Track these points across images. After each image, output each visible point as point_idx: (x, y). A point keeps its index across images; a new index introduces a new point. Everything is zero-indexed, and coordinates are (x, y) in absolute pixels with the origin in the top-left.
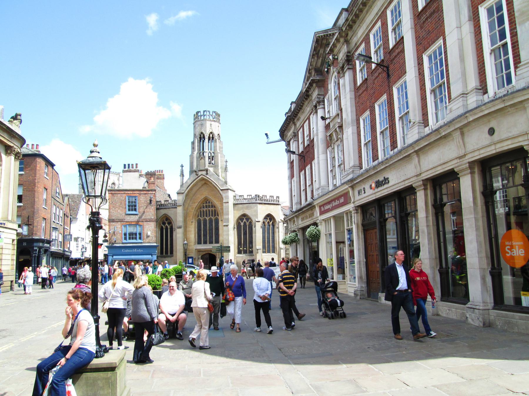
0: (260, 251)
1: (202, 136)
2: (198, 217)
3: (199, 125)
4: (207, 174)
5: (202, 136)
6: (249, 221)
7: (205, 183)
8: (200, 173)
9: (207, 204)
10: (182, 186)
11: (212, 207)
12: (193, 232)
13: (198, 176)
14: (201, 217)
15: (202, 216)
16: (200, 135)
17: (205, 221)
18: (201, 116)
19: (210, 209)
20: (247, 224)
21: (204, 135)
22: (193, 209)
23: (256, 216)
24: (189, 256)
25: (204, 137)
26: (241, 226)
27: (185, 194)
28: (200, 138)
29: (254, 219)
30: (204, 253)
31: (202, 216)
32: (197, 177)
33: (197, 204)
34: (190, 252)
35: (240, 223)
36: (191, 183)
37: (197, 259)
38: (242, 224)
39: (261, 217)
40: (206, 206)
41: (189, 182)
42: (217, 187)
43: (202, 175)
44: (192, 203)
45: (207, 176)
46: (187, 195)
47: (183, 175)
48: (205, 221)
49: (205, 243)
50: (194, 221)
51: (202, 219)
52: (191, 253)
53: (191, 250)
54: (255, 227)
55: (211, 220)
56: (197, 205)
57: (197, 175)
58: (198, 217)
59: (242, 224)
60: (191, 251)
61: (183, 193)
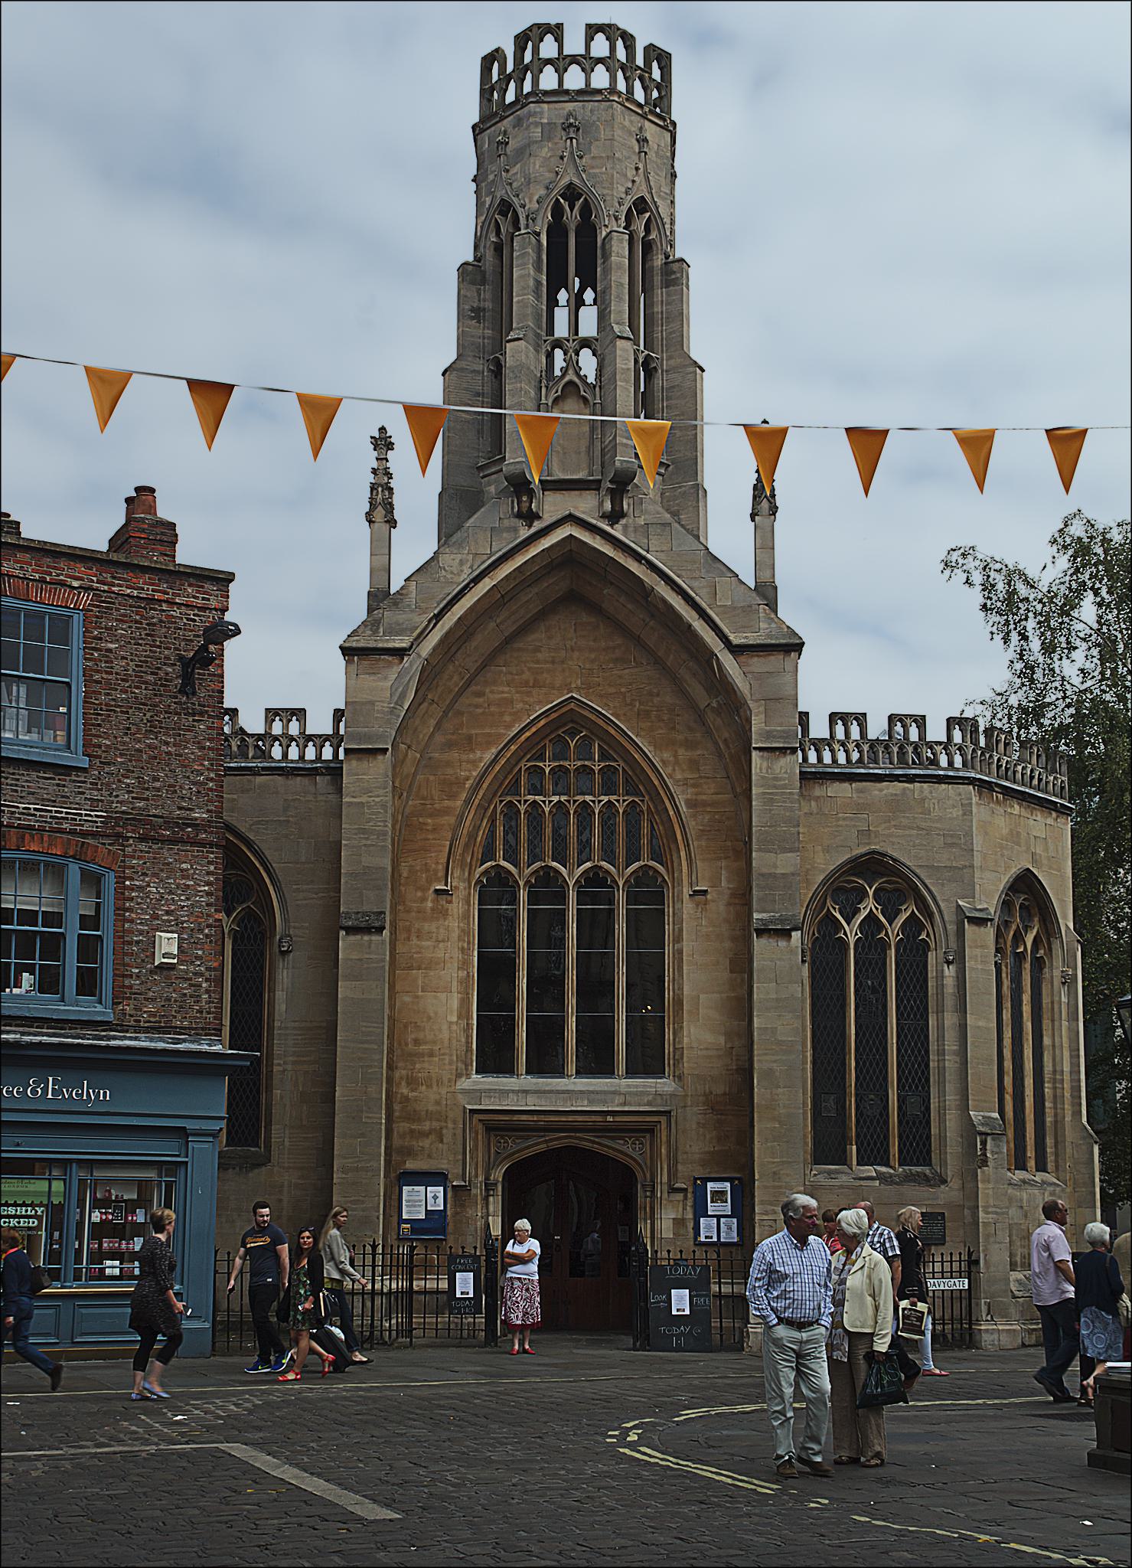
0: (998, 1151)
1: (572, 217)
2: (488, 854)
3: (548, 130)
4: (615, 516)
5: (572, 217)
6: (903, 917)
7: (573, 599)
8: (552, 506)
9: (572, 764)
10: (379, 597)
11: (609, 789)
12: (452, 974)
13: (537, 526)
14: (512, 856)
15: (524, 856)
16: (557, 211)
17: (547, 887)
18: (561, 63)
19: (597, 801)
20: (893, 932)
21: (586, 211)
22: (453, 796)
23: (963, 876)
24: (411, 1165)
25: (588, 228)
26: (844, 944)
27: (413, 665)
28: (557, 230)
29: (945, 898)
30: (536, 1145)
31: (524, 856)
32: (525, 533)
33: (488, 756)
34: (424, 1135)
35: (838, 927)
36: (476, 580)
37: (477, 1191)
38: (851, 933)
39: (988, 899)
40: (559, 772)
41: (459, 567)
42: (699, 625)
43: (570, 518)
44: (450, 745)
45: (617, 532)
46: (429, 675)
47: (389, 508)
48: (547, 887)
49: (545, 1061)
50: (457, 881)
51: (523, 874)
52: (426, 1143)
53: (430, 1116)
54: (959, 959)
55: (595, 885)
56: (494, 761)
57: (530, 517)
58: (488, 854)
59: (851, 933)
60: (427, 1126)
61: (400, 653)
